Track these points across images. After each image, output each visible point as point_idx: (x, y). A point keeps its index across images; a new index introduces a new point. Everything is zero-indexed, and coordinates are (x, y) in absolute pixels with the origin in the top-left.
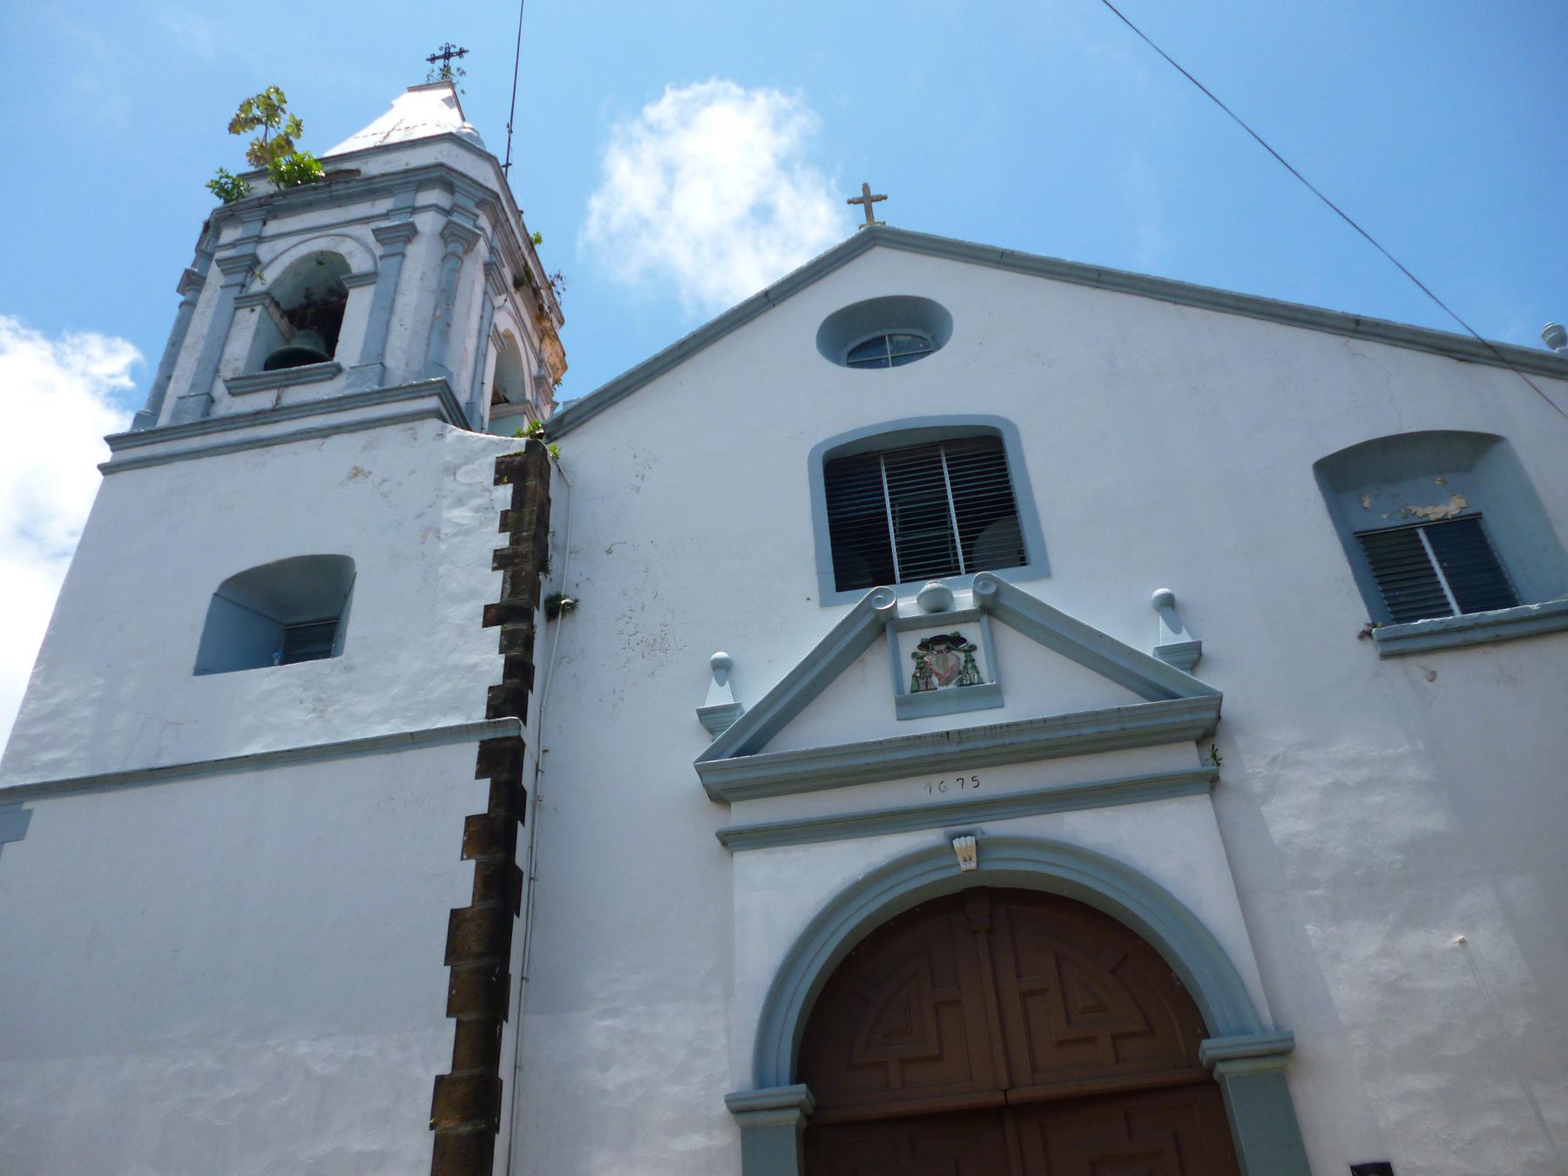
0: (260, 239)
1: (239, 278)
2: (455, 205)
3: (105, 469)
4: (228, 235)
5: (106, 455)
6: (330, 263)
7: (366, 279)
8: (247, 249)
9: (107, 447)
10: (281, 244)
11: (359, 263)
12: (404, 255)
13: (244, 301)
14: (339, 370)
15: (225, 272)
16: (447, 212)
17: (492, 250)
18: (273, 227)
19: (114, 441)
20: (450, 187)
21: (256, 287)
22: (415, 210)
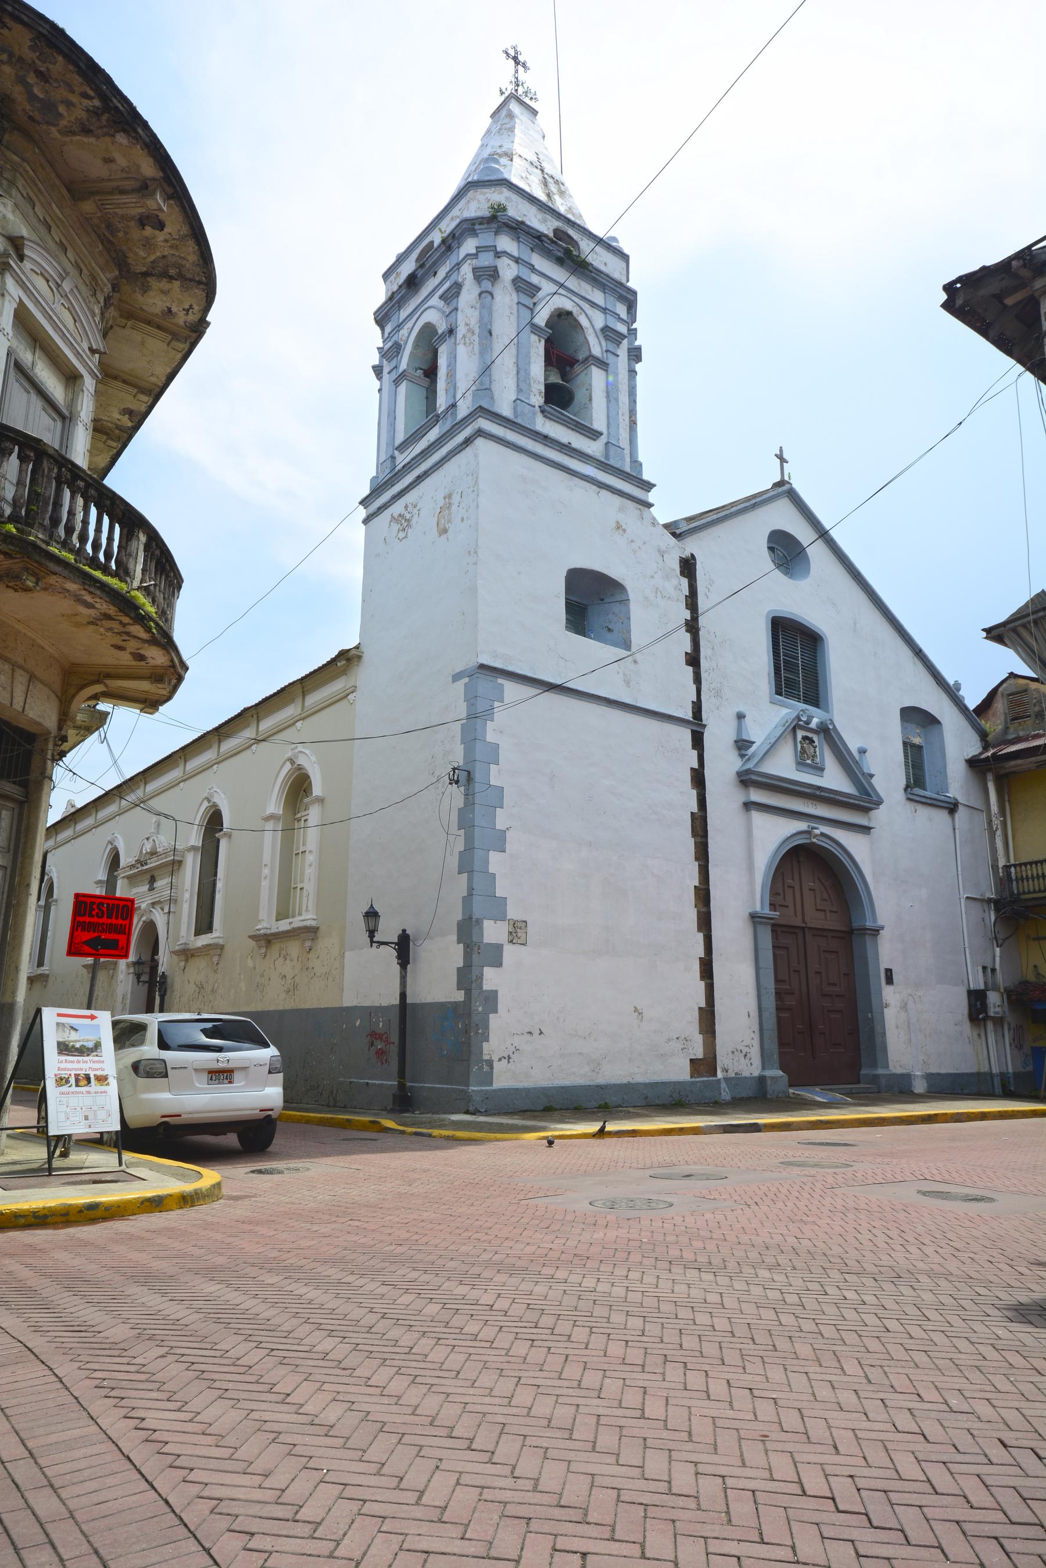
0: (399, 327)
1: (394, 363)
2: (477, 248)
3: (366, 521)
4: (388, 329)
5: (362, 513)
6: (429, 330)
7: (442, 338)
8: (393, 340)
9: (361, 507)
10: (410, 324)
11: (442, 328)
12: (456, 309)
13: (397, 382)
14: (438, 416)
15: (389, 360)
16: (475, 256)
17: (517, 260)
18: (404, 314)
19: (364, 502)
20: (474, 233)
21: (403, 366)
22: (458, 265)
